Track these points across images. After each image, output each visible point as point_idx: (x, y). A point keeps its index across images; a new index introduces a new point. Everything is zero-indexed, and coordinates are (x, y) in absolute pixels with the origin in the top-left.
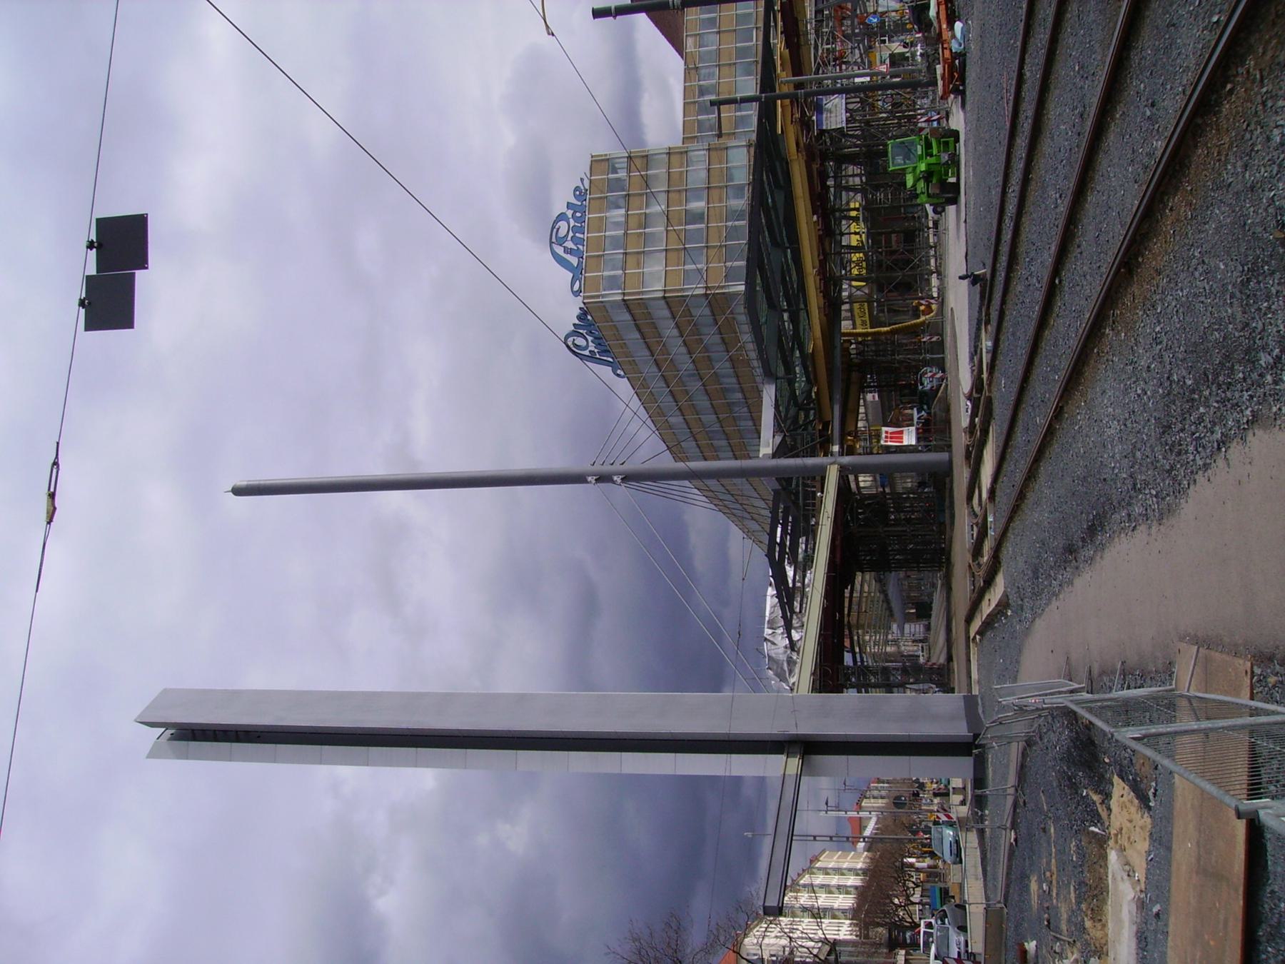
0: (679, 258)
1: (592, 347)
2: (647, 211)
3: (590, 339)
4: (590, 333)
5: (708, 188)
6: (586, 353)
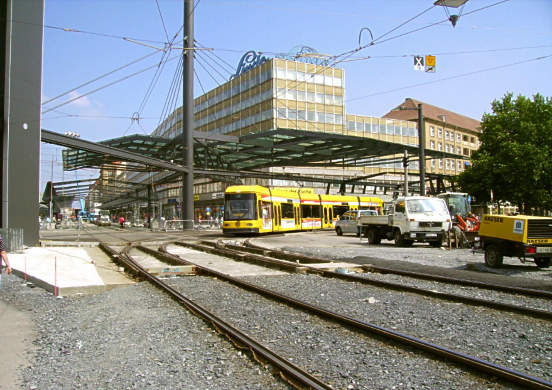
0: (292, 107)
1: (248, 64)
2: (315, 94)
3: (252, 64)
4: (255, 63)
5: (325, 124)
6: (244, 62)
